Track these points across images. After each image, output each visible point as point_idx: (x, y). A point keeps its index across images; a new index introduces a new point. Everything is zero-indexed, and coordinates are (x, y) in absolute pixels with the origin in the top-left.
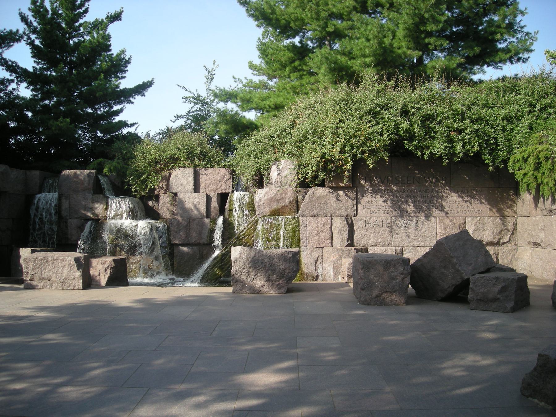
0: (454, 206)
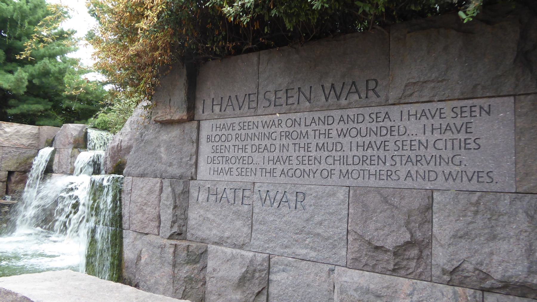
0: (398, 159)
